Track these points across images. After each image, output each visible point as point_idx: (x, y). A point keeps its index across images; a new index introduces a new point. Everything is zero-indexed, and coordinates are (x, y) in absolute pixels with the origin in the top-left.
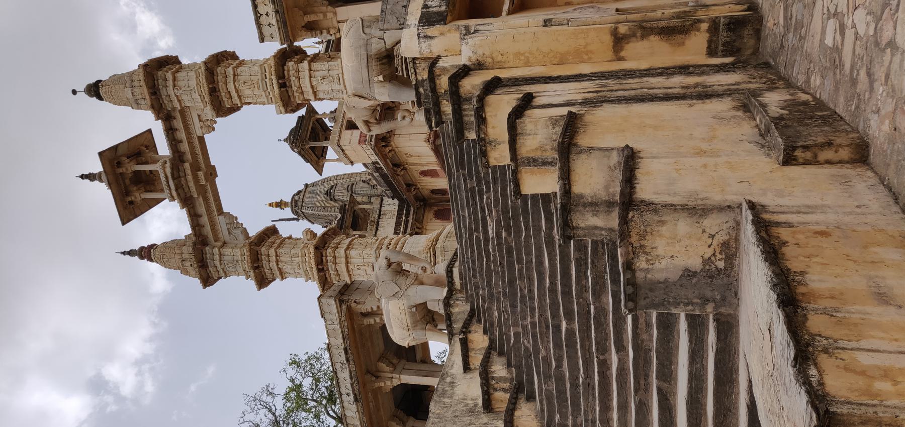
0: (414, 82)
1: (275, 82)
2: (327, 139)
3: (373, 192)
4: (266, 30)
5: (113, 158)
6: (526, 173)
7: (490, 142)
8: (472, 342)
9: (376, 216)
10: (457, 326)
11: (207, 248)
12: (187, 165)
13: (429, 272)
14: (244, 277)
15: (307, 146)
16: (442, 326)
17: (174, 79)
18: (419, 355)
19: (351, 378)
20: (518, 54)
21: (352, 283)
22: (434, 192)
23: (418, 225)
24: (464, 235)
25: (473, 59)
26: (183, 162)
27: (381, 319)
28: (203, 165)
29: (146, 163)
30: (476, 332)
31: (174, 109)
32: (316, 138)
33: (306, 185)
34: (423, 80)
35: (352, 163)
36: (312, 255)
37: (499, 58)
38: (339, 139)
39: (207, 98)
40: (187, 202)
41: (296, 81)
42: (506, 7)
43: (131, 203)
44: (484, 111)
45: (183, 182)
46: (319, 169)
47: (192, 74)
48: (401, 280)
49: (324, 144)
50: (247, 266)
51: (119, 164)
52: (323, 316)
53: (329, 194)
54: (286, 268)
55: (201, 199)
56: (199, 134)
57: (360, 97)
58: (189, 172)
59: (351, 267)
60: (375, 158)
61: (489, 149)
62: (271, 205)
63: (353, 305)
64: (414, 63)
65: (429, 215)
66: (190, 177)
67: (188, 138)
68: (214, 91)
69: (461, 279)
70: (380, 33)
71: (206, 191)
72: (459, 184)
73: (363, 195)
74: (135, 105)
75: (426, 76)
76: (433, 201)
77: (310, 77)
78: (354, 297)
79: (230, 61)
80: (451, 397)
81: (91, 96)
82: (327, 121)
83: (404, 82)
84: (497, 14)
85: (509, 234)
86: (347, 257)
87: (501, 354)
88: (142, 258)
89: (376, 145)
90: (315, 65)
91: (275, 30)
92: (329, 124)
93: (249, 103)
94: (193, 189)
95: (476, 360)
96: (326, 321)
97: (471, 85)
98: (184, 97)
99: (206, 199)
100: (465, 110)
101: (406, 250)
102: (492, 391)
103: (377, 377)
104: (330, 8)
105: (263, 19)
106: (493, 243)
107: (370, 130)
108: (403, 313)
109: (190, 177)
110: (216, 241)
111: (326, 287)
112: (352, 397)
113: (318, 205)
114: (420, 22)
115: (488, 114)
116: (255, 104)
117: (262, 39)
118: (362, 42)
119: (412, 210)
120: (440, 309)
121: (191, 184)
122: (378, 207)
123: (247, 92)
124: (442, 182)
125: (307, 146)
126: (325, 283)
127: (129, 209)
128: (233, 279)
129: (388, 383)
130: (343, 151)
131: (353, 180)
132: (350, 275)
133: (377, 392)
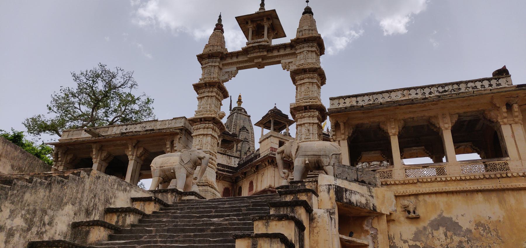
0: (304, 180)
1: (308, 104)
2: (275, 130)
3: (243, 153)
4: (336, 101)
5: (272, 16)
6: (248, 243)
7: (267, 222)
8: (149, 204)
9: (229, 154)
10: (160, 196)
11: (219, 60)
12: (265, 53)
13: (194, 181)
14: (201, 77)
15: (271, 119)
16: (160, 187)
17: (312, 51)
18: (144, 172)
19: (136, 132)
20: (317, 242)
21: (192, 137)
22: (240, 189)
23: (221, 178)
24: (214, 203)
25: (315, 216)
26: (268, 52)
27: (169, 152)
28: (265, 62)
29: (268, 33)
30: (155, 207)
31: (296, 50)
32: (275, 124)
33: (249, 116)
34: (305, 186)
35: (260, 142)
36: (210, 116)
37: (315, 231)
39: (301, 67)
40: (245, 51)
41: (307, 116)
42: (344, 237)
43: (247, 23)
44: (286, 220)
45: (257, 50)
46: (258, 124)
47: (314, 61)
48: (190, 165)
49: (272, 128)
50: (207, 80)
51: (268, 19)
52: (174, 119)
53: (244, 128)
54: (204, 101)
55: (246, 59)
56: (282, 61)
57: (297, 150)
58: (262, 54)
59: (201, 137)
60: (262, 155)
61: (264, 221)
62: (240, 96)
63: (179, 136)
64: (315, 181)
66: (259, 54)
67: (280, 55)
68: (304, 71)
69: (188, 200)
70: (332, 163)
71: (250, 62)
72: (244, 203)
73: (241, 147)
74: (299, 30)
75: (307, 187)
77: (310, 123)
78: (184, 138)
79: (320, 81)
80: (117, 189)
81: (305, 9)
82: (285, 131)
83: (304, 175)
84: (341, 231)
85: (212, 231)
86: (207, 135)
87: (140, 221)
88: (217, 25)
90: (316, 126)
91: (336, 106)
92: (283, 132)
93: (297, 89)
94: (252, 55)
95: (138, 206)
96: (171, 120)
97: (301, 214)
98: (302, 56)
99: (246, 61)
100: (287, 209)
101: (208, 169)
102: (118, 214)
103: (134, 147)
104: (347, 137)
105: (342, 101)
106: (208, 221)
107: (278, 153)
108: (171, 164)
109: (259, 54)
110: (223, 64)
111: (191, 122)
112: (125, 131)
113: (238, 122)
114: (338, 186)
115: (284, 222)
116: (297, 93)
117: (331, 99)
118: (328, 153)
119: (231, 175)
120: (171, 186)
121: (255, 55)
123: (303, 88)
124: (245, 193)
125: (271, 119)
126: (193, 121)
127: (244, 22)
128: (201, 71)
129: (130, 153)
130: (267, 138)
131: (251, 142)
132: (196, 136)
133: (126, 146)
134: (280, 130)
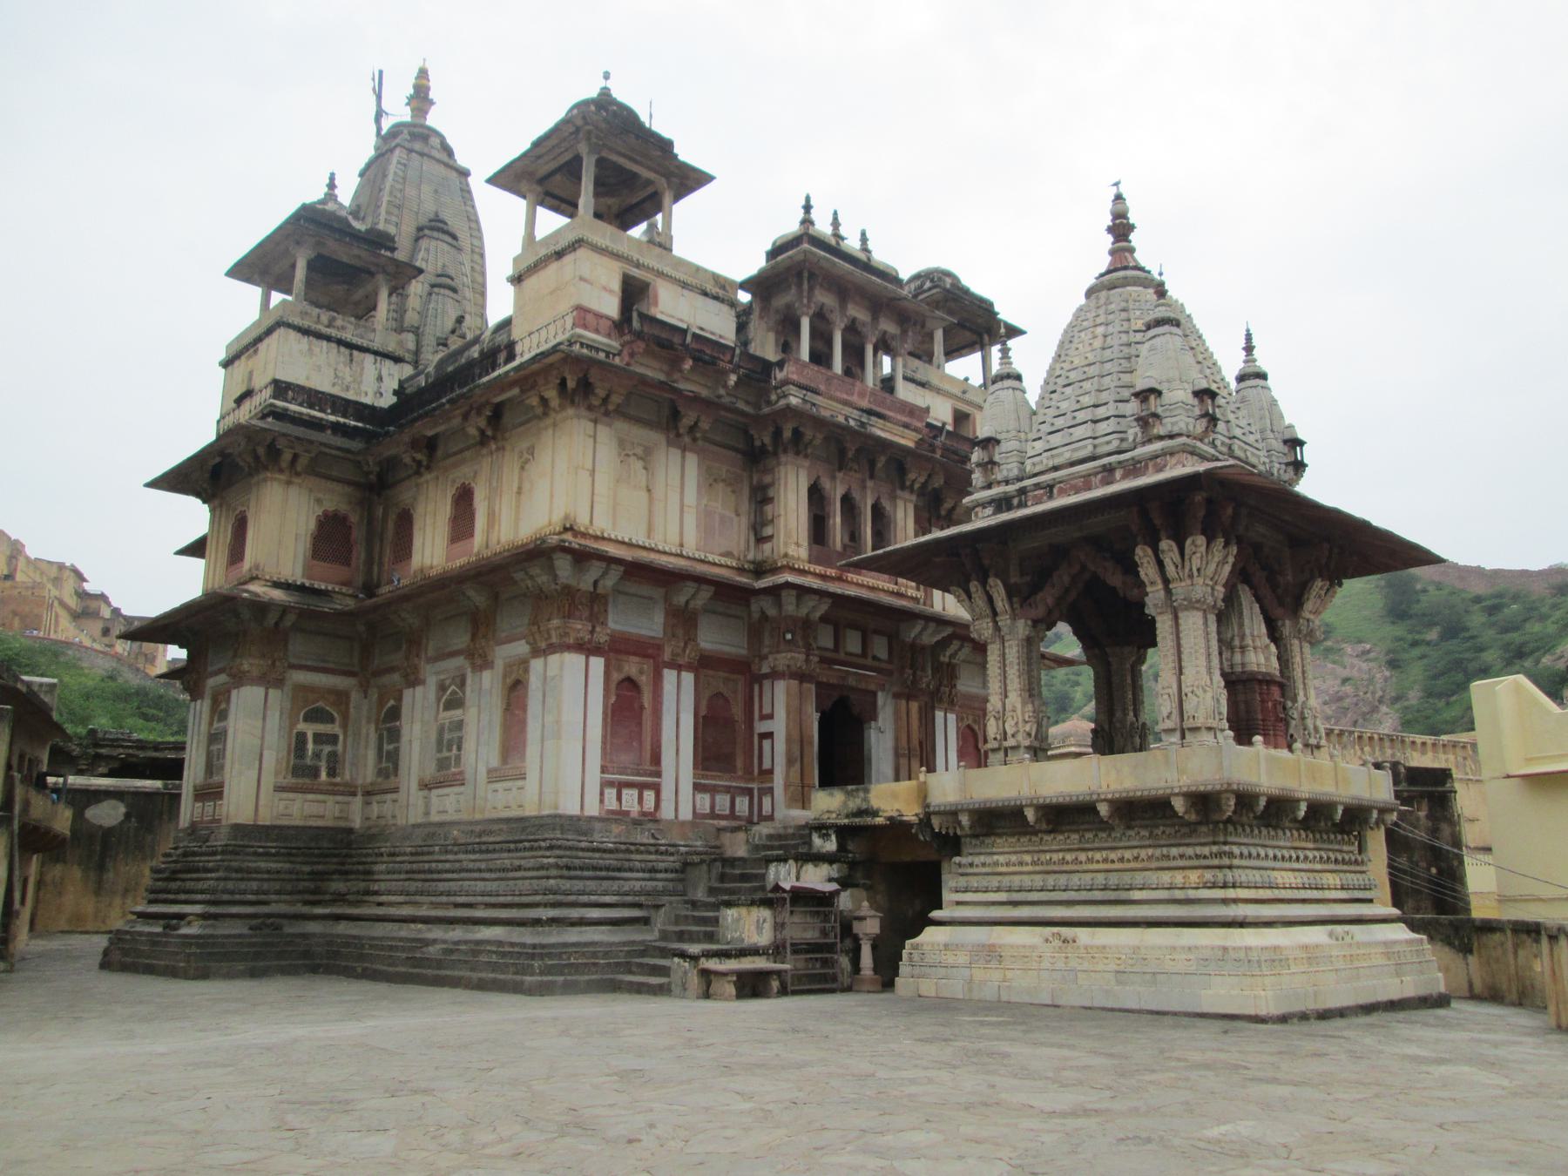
3: (429, 341)
9: (347, 336)
15: (583, 148)
22: (405, 522)
23: (303, 461)
35: (517, 280)
38: (596, 248)
46: (509, 178)
49: (586, 200)
60: (526, 351)
62: (423, 74)
65: (335, 499)
73: (423, 314)
76: (380, 511)
89: (571, 360)
92: (638, 232)
113: (411, 192)
122: (376, 346)
124: (432, 550)
125: (583, 148)
130: (559, 255)
131: (468, 294)
134: (624, 219)
